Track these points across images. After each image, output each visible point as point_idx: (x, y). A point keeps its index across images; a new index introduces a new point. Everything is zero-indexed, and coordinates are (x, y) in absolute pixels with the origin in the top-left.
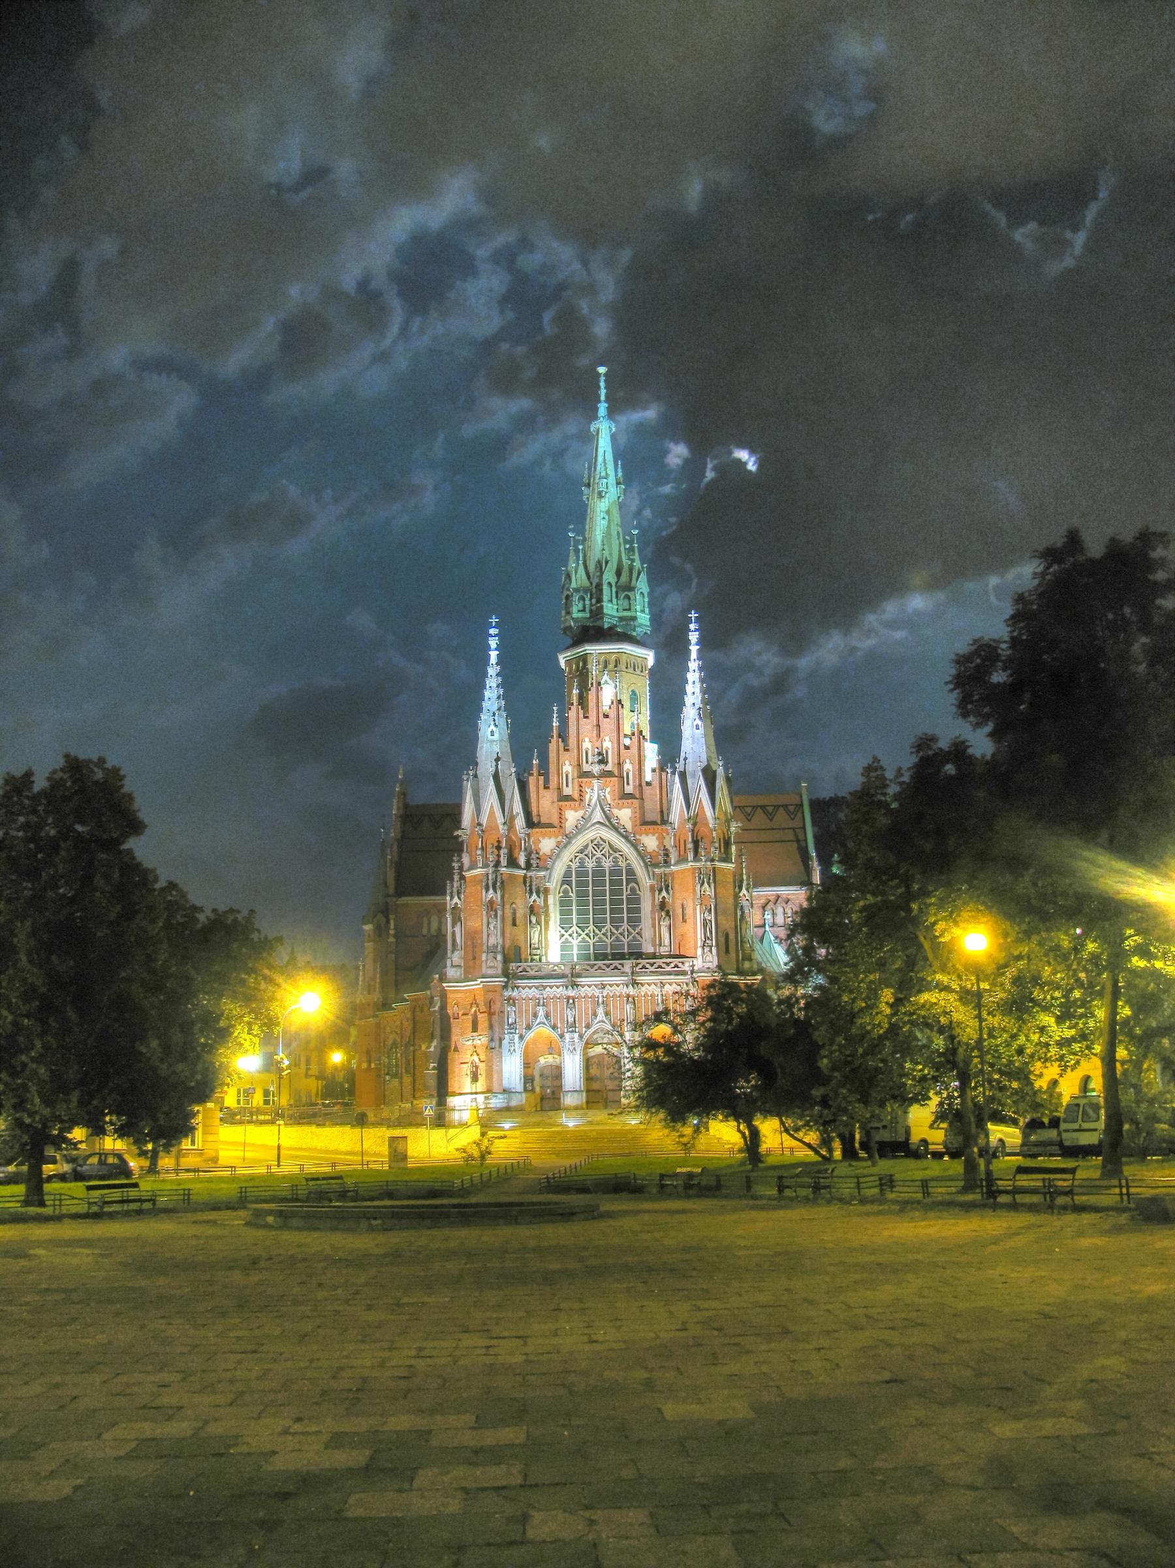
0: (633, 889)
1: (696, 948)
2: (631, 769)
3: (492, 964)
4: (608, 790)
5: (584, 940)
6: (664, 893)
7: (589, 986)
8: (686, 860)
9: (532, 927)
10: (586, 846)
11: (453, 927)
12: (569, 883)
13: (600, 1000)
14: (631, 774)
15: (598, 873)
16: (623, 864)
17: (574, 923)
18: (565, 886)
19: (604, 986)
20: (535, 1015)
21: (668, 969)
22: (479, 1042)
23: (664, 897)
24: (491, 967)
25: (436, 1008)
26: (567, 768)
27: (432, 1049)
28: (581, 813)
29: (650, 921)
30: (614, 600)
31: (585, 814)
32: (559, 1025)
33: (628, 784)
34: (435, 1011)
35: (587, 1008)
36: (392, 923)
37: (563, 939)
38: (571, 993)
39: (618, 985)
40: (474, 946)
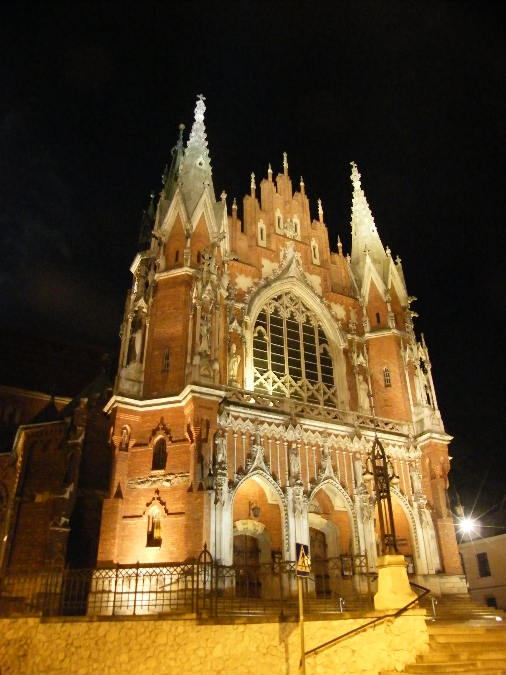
0: (325, 350)
2: (317, 246)
3: (207, 373)
5: (279, 389)
7: (314, 432)
8: (386, 328)
9: (231, 357)
10: (280, 297)
12: (265, 326)
13: (326, 451)
14: (317, 250)
15: (293, 325)
16: (313, 323)
17: (270, 367)
18: (260, 328)
19: (330, 434)
20: (250, 457)
22: (167, 484)
25: (80, 441)
26: (261, 224)
27: (67, 496)
29: (346, 383)
32: (279, 476)
34: (77, 444)
35: (311, 459)
37: (257, 383)
38: (291, 435)
39: (343, 437)
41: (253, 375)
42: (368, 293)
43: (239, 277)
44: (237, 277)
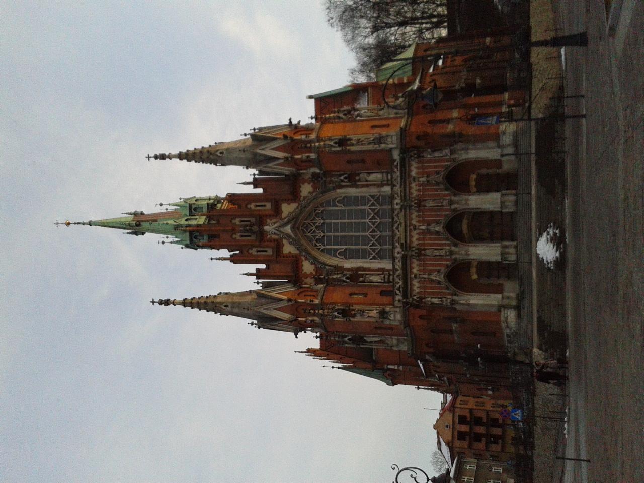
1: (382, 151)
3: (392, 316)
4: (268, 221)
6: (342, 178)
11: (367, 342)
21: (399, 173)
23: (345, 178)
24: (395, 316)
28: (285, 242)
29: (364, 189)
30: (196, 217)
31: (285, 238)
33: (265, 206)
35: (430, 239)
36: (389, 367)
40: (381, 328)
41: (373, 260)
42: (286, 168)
43: (305, 271)
44: (306, 273)
